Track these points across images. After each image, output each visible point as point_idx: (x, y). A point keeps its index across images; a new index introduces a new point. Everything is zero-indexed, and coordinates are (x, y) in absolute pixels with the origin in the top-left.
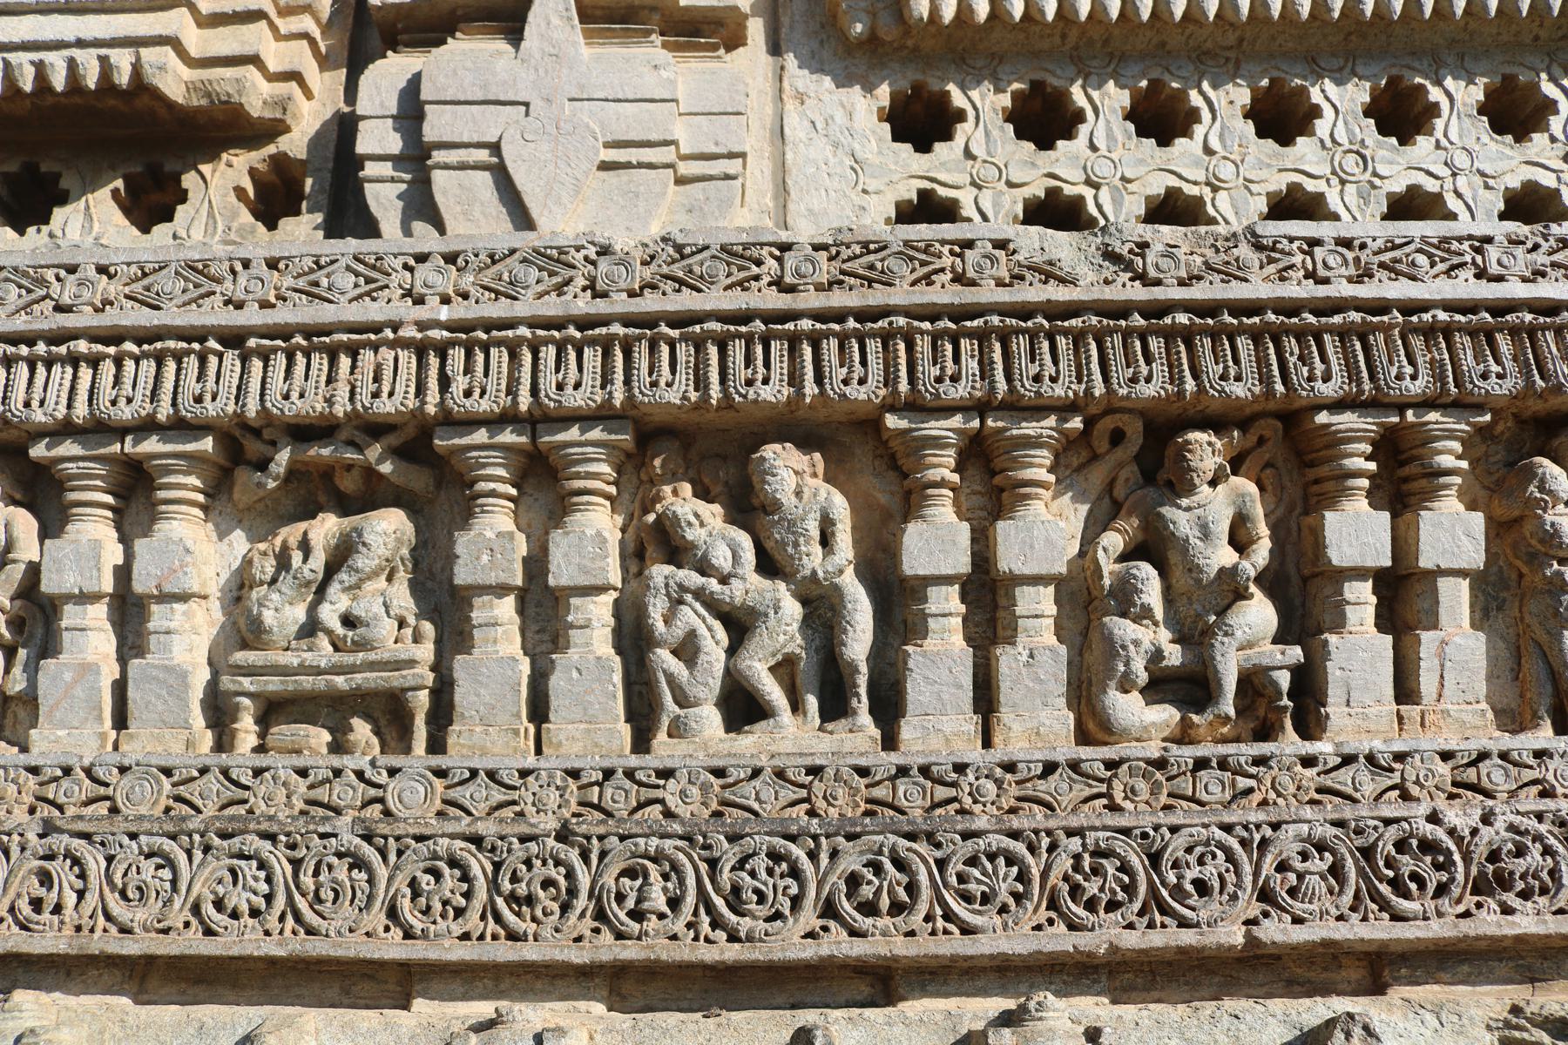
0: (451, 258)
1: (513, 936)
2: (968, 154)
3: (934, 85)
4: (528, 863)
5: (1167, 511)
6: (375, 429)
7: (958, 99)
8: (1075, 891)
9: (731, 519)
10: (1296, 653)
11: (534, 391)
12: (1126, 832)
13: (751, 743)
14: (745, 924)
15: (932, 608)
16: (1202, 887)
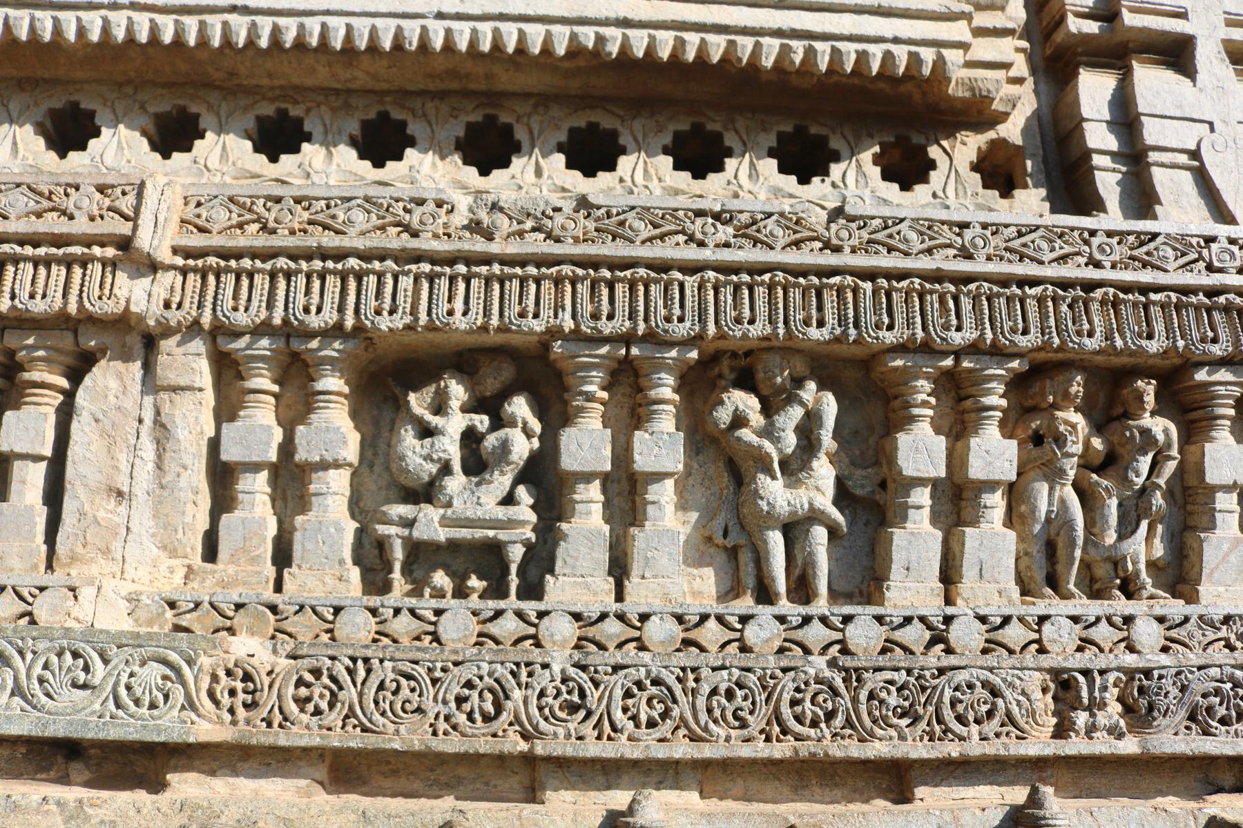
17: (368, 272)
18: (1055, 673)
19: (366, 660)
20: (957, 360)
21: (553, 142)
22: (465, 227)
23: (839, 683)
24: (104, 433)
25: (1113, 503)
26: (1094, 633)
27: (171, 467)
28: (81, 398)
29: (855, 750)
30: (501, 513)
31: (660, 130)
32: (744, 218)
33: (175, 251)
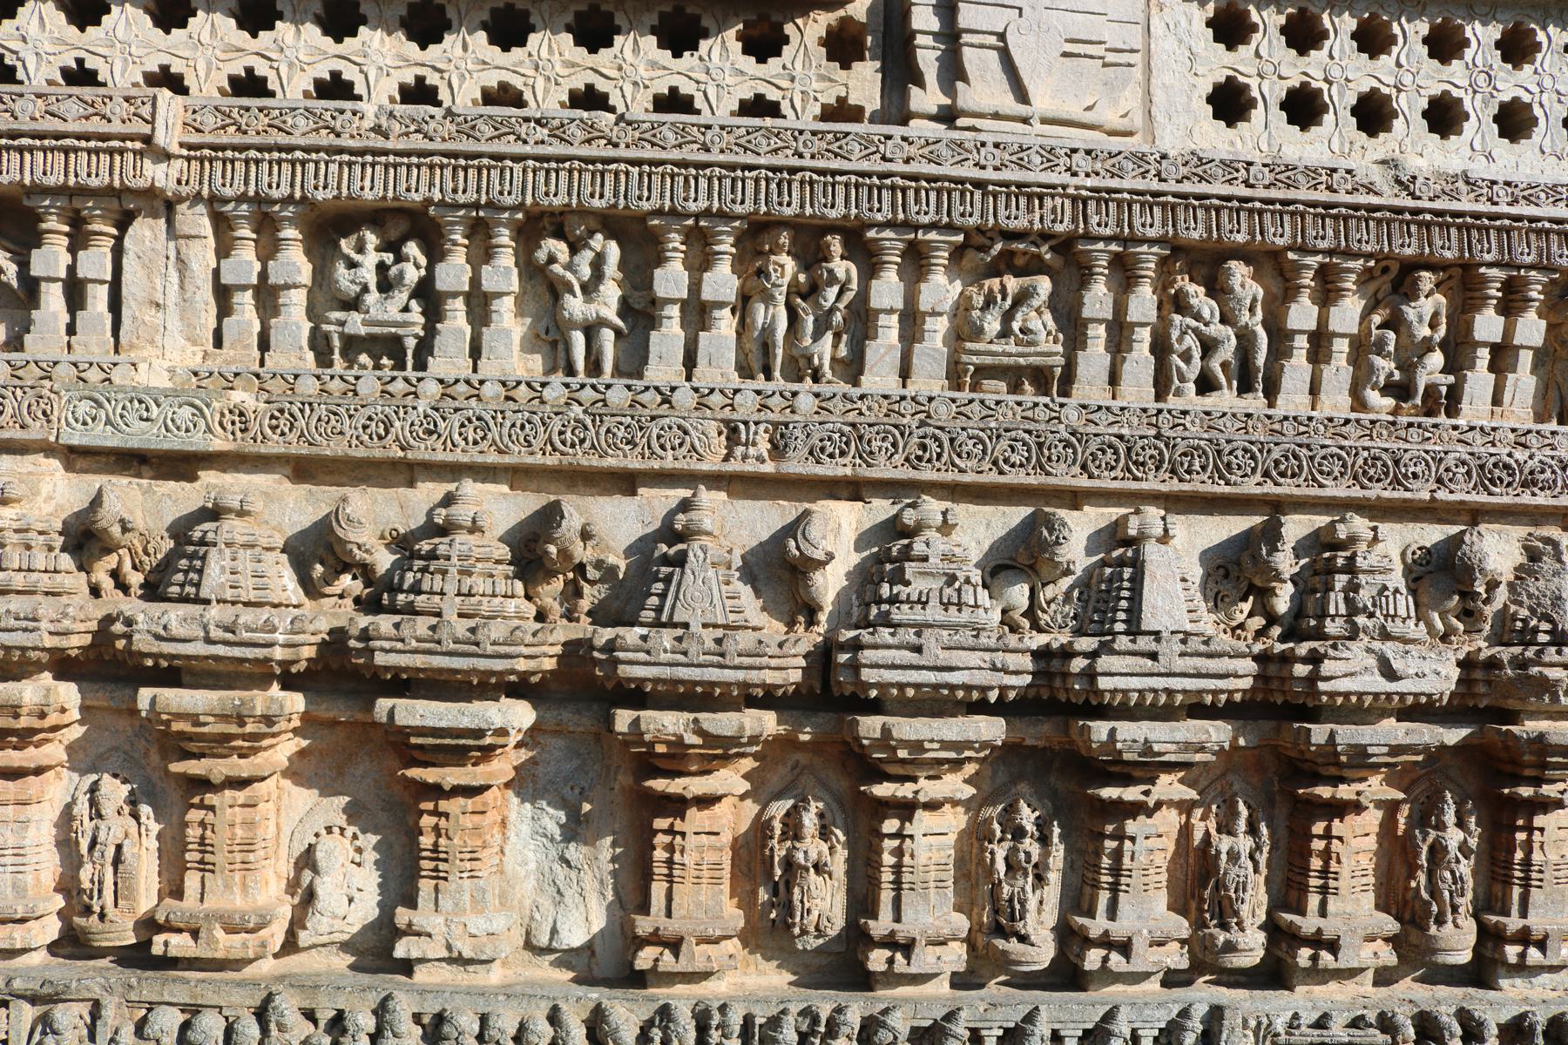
0: (1088, 152)
1: (1136, 479)
2: (1258, 55)
3: (1241, 7)
4: (1143, 449)
5: (1404, 308)
6: (1045, 236)
7: (1255, 17)
8: (1365, 473)
9: (1207, 295)
10: (1451, 379)
11: (1130, 226)
12: (1386, 450)
13: (1211, 401)
14: (1233, 478)
15: (1296, 344)
16: (1415, 476)
17: (309, 161)
18: (727, 422)
19: (310, 404)
20: (697, 222)
21: (477, 21)
22: (372, 129)
23: (588, 422)
24: (144, 266)
25: (811, 319)
26: (771, 402)
27: (189, 288)
28: (127, 242)
29: (595, 461)
30: (400, 317)
31: (564, 9)
32: (556, 123)
33: (181, 145)
